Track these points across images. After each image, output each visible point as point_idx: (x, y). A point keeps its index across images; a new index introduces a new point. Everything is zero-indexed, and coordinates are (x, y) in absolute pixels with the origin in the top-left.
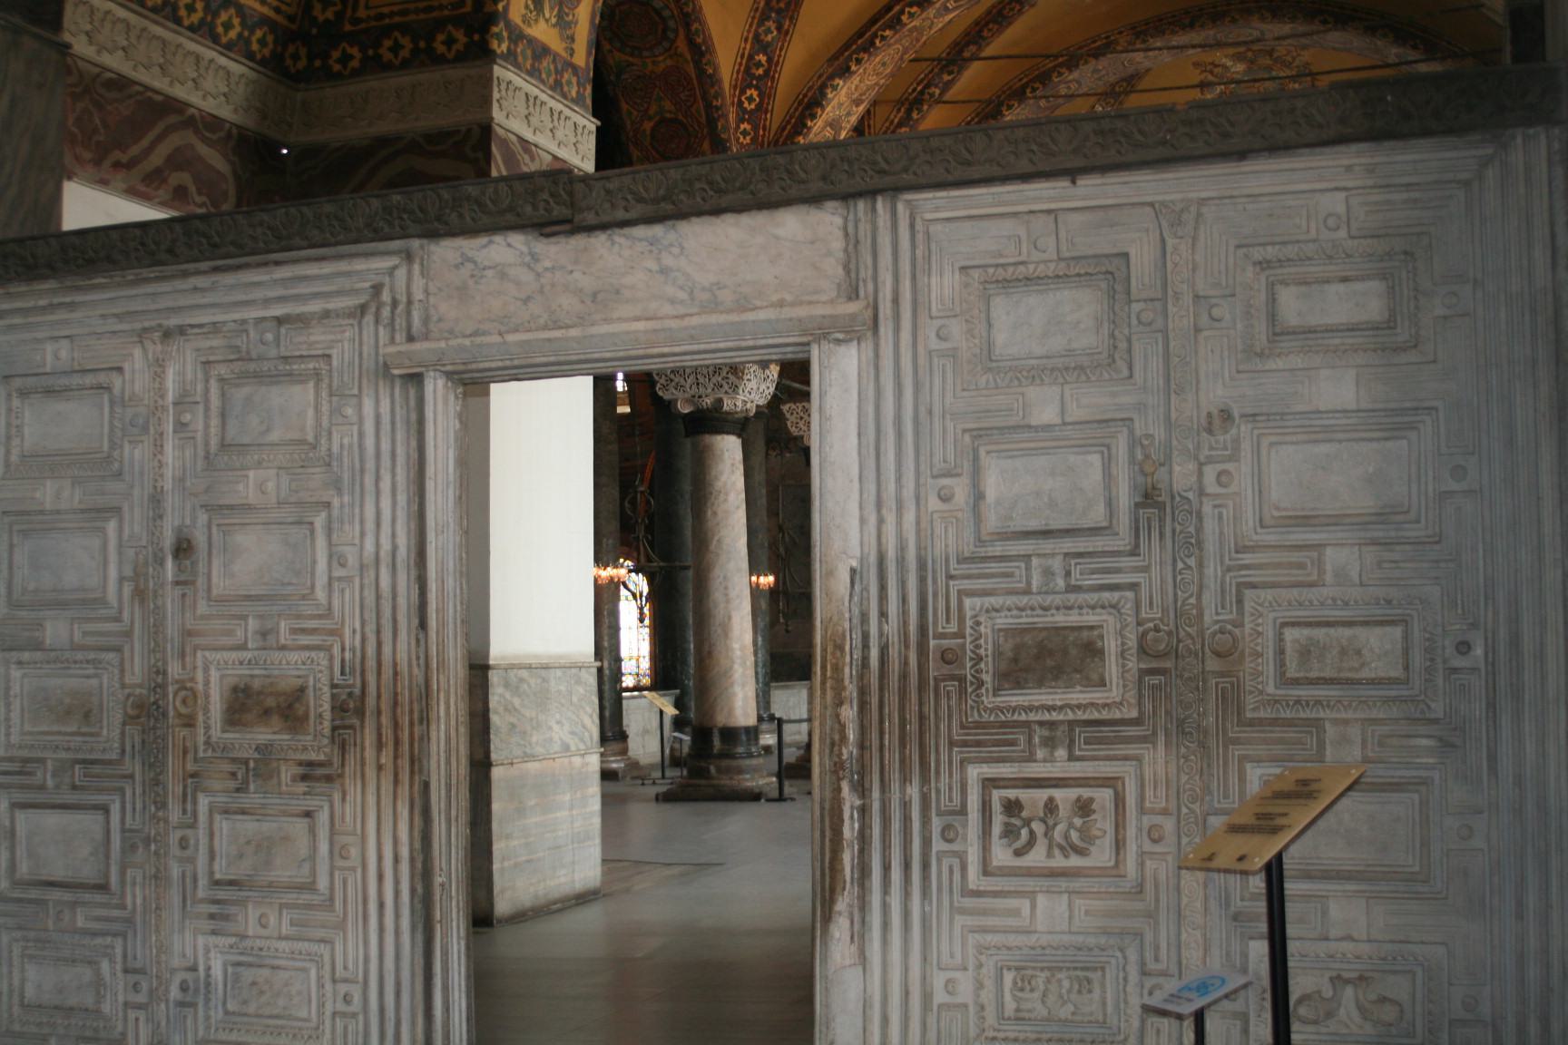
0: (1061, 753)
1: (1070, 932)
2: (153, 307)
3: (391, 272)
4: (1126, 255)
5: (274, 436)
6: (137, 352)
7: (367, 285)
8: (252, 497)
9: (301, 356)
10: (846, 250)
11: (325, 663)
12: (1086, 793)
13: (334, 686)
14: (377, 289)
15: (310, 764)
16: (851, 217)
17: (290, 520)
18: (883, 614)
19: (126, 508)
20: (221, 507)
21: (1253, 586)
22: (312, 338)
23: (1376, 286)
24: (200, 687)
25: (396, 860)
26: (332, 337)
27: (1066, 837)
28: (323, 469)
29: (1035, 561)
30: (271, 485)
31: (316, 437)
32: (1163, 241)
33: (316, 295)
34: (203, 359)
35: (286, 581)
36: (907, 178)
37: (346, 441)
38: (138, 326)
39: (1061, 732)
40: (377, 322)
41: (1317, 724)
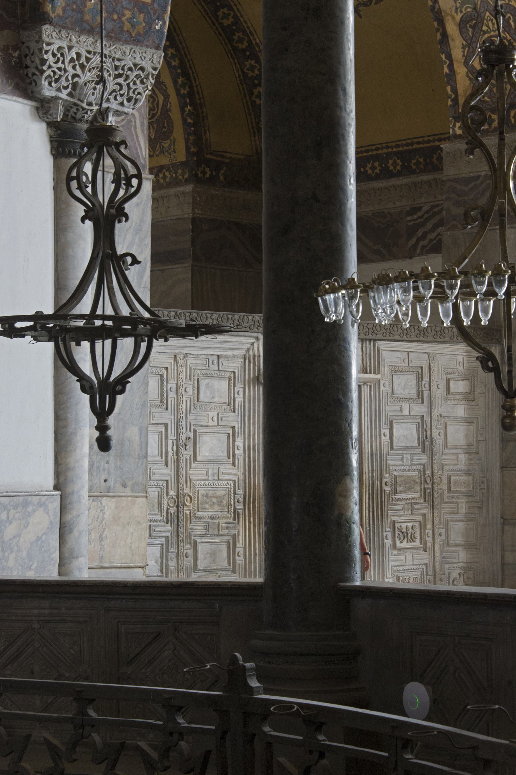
0: (410, 512)
1: (413, 565)
2: (178, 345)
3: (252, 344)
4: (422, 368)
5: (216, 400)
6: (172, 361)
7: (246, 347)
8: (211, 423)
9: (226, 371)
10: (362, 355)
11: (232, 485)
12: (414, 524)
13: (235, 493)
14: (248, 350)
15: (229, 523)
16: (364, 345)
17: (222, 432)
18: (373, 470)
19: (169, 424)
20: (198, 425)
21: (446, 465)
22: (230, 365)
23: (466, 383)
24: (191, 495)
25: (255, 554)
26: (236, 365)
27: (411, 537)
28: (233, 414)
29: (405, 456)
30: (215, 418)
31: (229, 401)
32: (429, 364)
33: (230, 349)
34: (194, 368)
35: (219, 455)
36: (382, 337)
37: (240, 404)
38: (173, 351)
39: (410, 507)
40: (249, 362)
41: (457, 503)
